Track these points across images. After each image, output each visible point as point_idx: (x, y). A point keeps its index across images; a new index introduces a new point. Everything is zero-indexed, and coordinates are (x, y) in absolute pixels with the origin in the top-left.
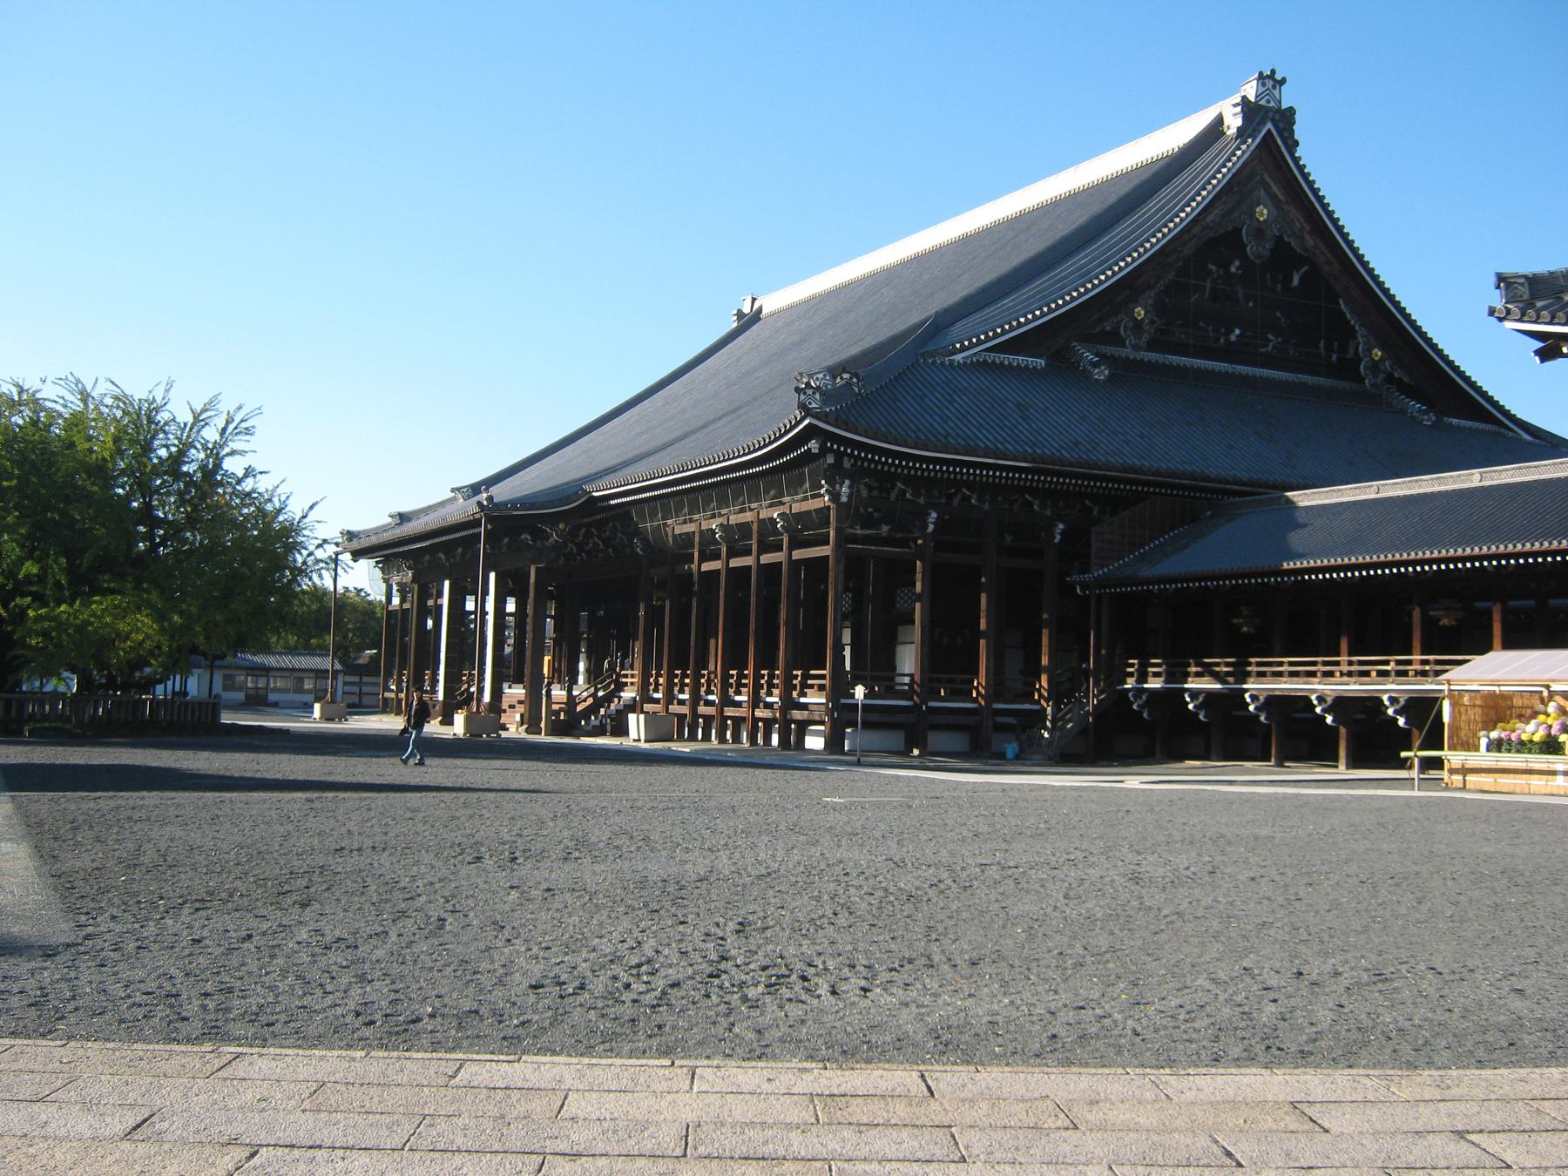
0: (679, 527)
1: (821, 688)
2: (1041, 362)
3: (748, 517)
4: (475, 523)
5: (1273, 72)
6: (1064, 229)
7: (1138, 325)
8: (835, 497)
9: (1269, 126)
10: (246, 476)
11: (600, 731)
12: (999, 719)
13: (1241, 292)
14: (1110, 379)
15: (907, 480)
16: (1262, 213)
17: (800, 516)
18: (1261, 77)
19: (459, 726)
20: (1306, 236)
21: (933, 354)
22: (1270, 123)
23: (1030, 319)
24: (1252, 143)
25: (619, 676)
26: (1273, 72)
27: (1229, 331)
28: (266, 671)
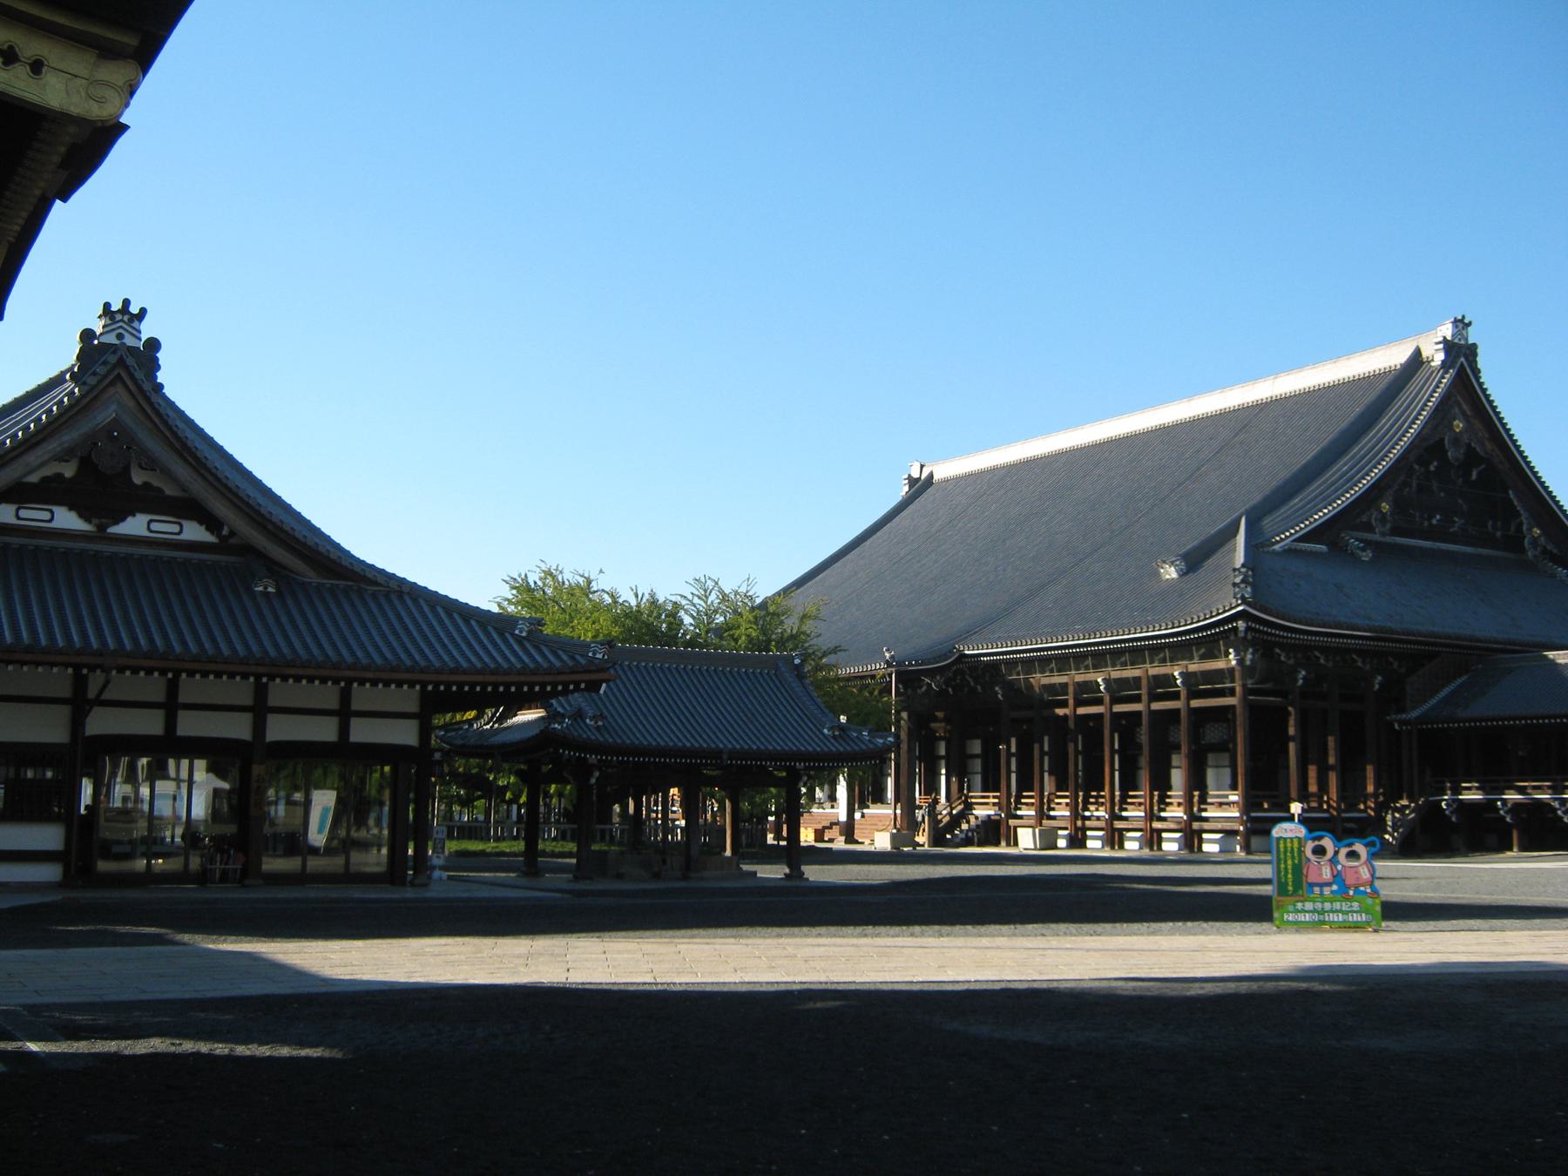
0: (1041, 679)
1: (1179, 804)
3: (1136, 673)
7: (1384, 515)
8: (1241, 662)
11: (968, 842)
13: (1435, 485)
15: (1282, 646)
16: (1459, 425)
17: (1204, 673)
18: (1456, 322)
22: (1461, 354)
23: (1321, 516)
25: (967, 797)
27: (1430, 519)
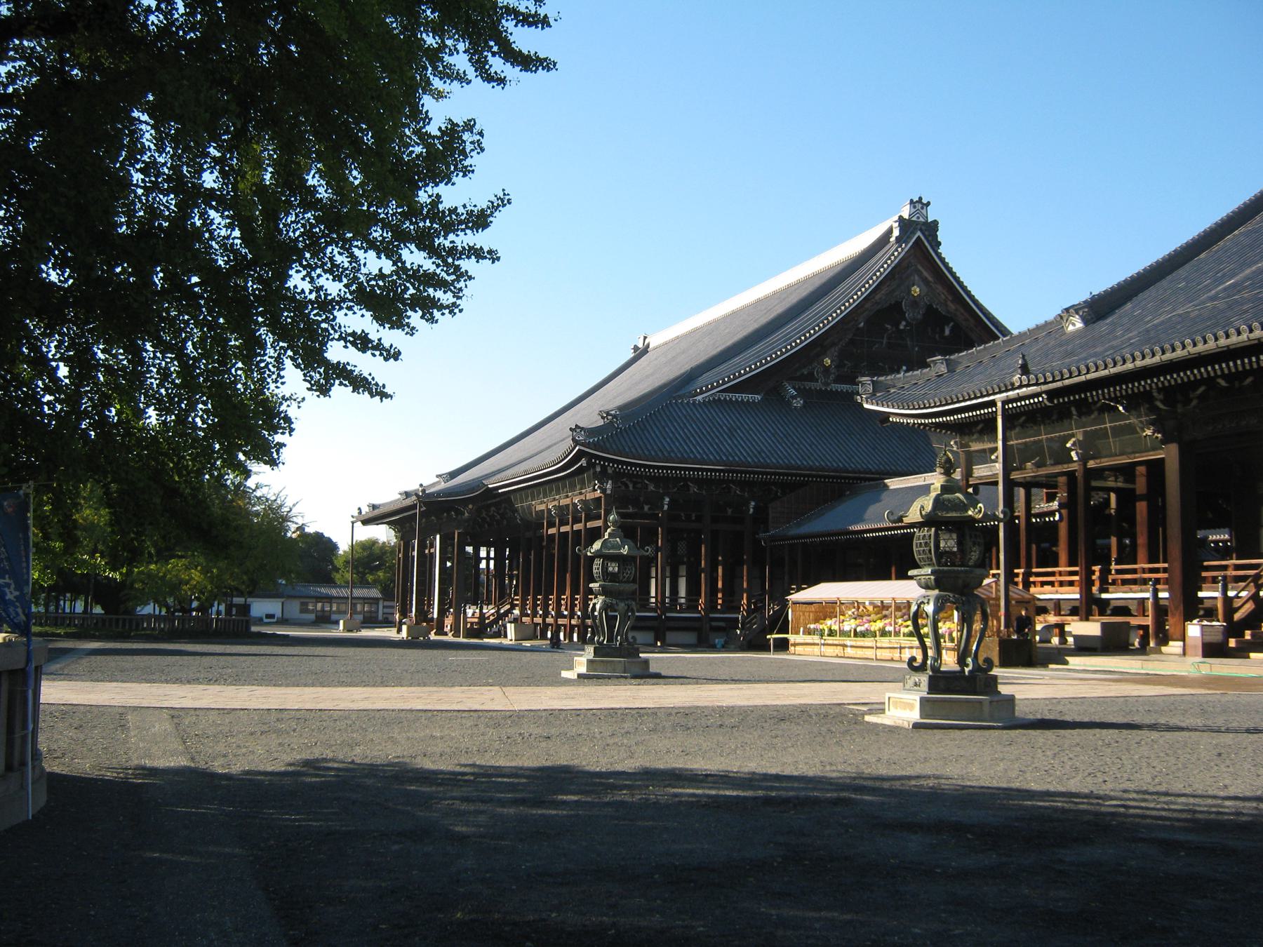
2: (758, 397)
4: (413, 507)
5: (920, 198)
6: (779, 309)
8: (604, 491)
9: (919, 234)
10: (257, 488)
12: (714, 624)
14: (804, 406)
16: (916, 290)
19: (404, 634)
20: (950, 304)
21: (680, 397)
24: (906, 247)
26: (920, 198)
28: (330, 599)
